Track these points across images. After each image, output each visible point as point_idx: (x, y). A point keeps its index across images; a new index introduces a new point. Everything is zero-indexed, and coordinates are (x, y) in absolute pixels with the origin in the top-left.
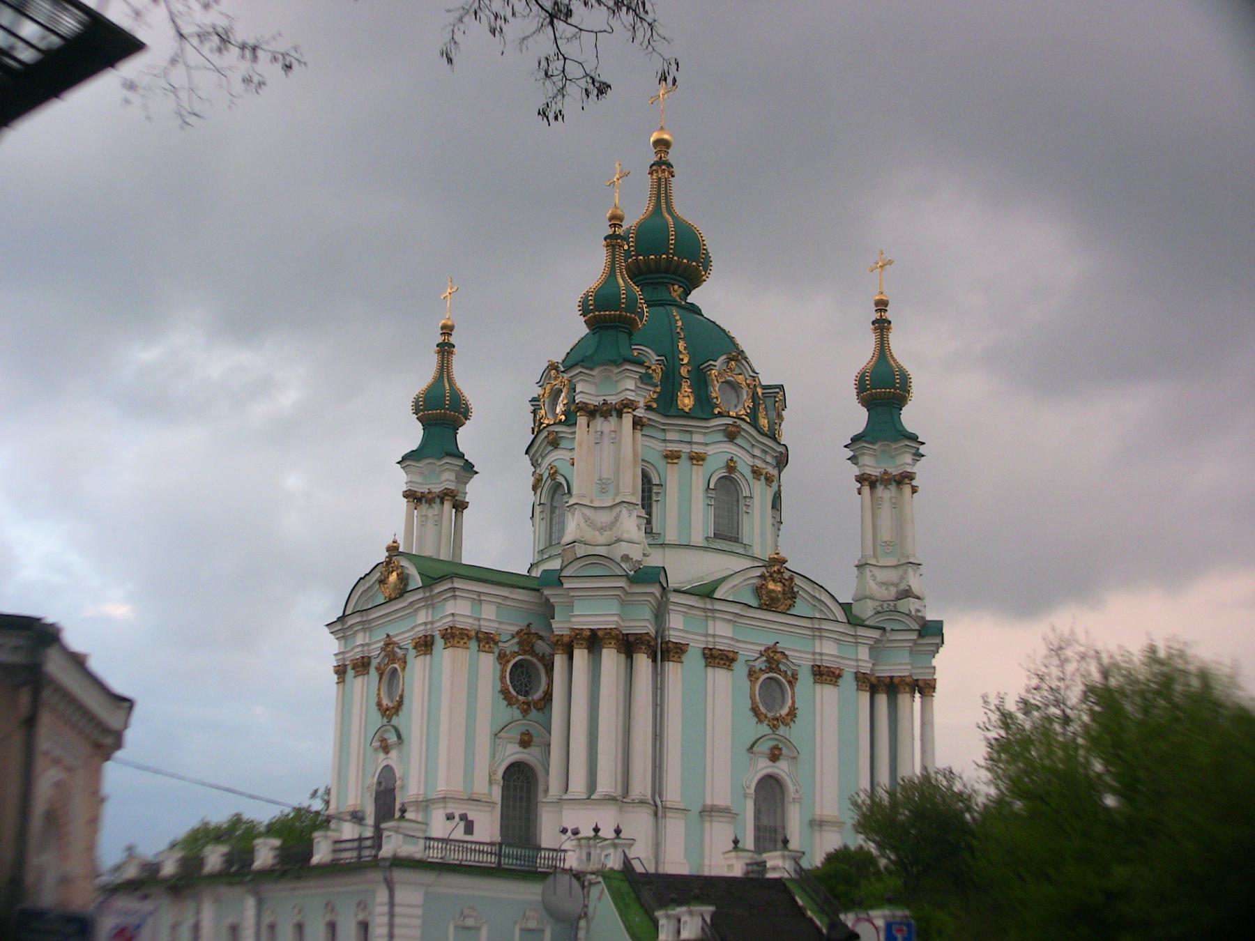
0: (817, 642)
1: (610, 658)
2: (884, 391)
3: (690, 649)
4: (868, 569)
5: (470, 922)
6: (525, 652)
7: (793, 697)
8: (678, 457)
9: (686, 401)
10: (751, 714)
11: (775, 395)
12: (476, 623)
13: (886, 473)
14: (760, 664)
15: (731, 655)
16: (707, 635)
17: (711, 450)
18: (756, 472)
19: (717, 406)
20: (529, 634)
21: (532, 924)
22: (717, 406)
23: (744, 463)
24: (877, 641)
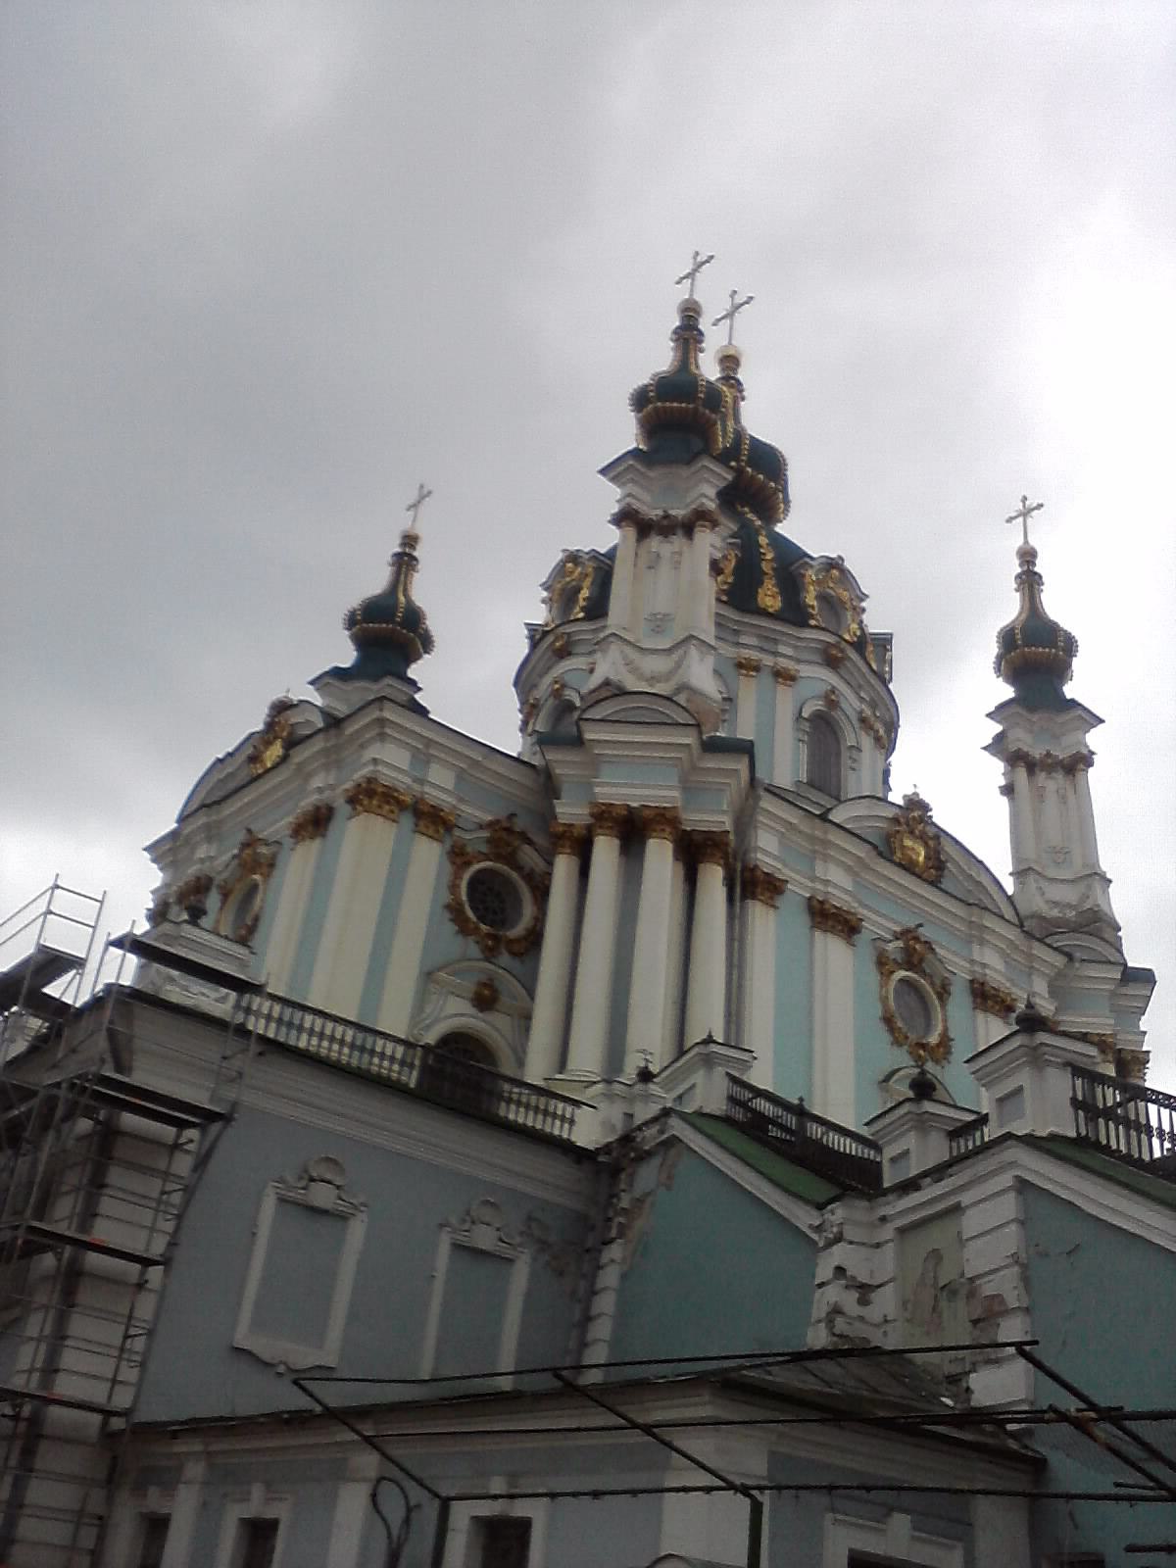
0: (976, 948)
1: (660, 854)
2: (1036, 657)
3: (787, 893)
4: (1031, 878)
5: (322, 1196)
6: (498, 857)
7: (945, 1021)
8: (757, 669)
9: (769, 597)
10: (882, 1028)
11: (884, 642)
12: (416, 787)
13: (1048, 755)
14: (893, 947)
15: (854, 922)
16: (814, 879)
17: (805, 670)
18: (863, 720)
19: (812, 617)
20: (509, 830)
21: (484, 1238)
22: (812, 617)
23: (851, 703)
24: (1060, 974)
